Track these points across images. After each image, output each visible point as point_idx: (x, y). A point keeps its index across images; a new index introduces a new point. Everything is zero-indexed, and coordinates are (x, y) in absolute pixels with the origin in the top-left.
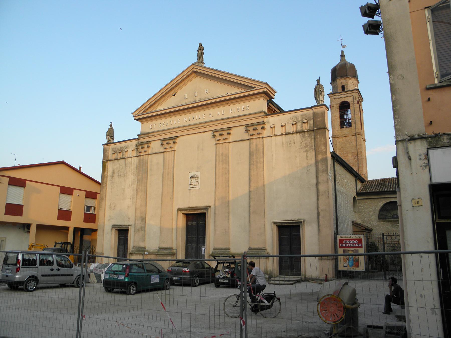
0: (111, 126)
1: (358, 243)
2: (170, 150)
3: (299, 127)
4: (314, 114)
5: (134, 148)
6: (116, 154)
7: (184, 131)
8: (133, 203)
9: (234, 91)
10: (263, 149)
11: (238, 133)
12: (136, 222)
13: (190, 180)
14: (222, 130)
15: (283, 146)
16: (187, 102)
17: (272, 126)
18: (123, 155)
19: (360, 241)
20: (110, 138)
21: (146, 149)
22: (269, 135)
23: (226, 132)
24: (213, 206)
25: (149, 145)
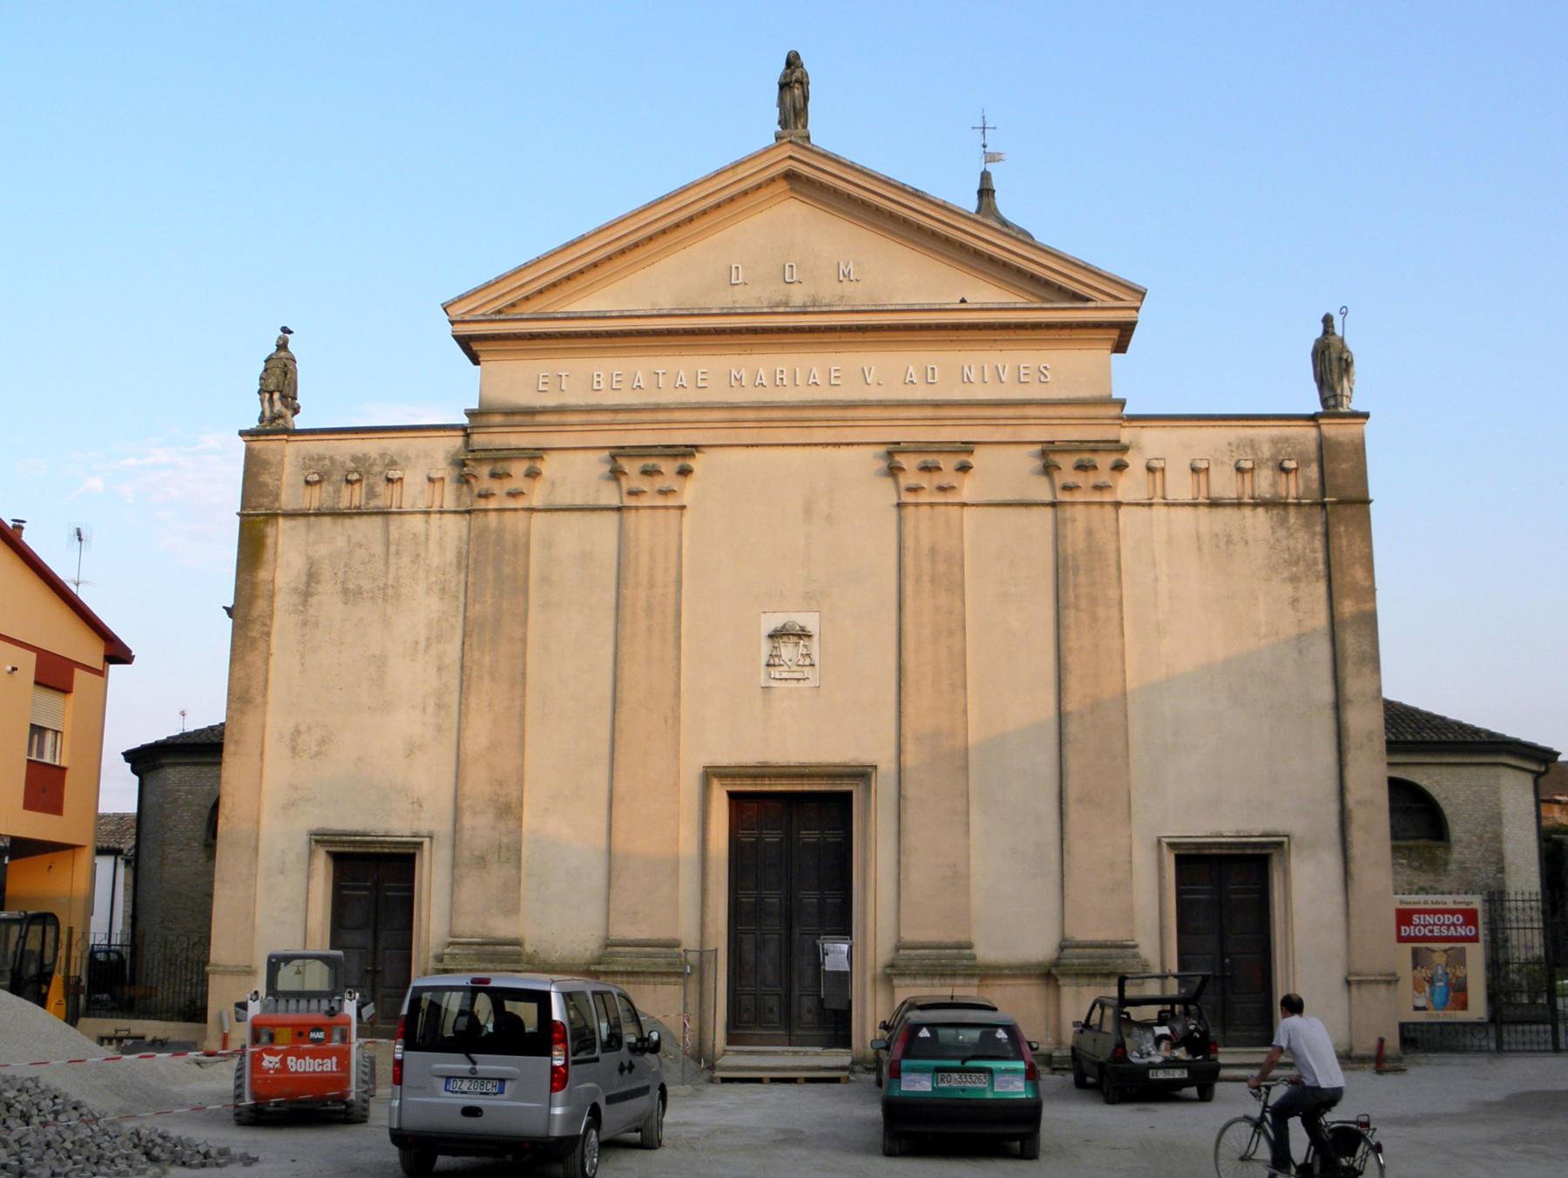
0: (282, 346)
1: (1466, 924)
2: (660, 501)
3: (1264, 483)
4: (1322, 443)
5: (443, 470)
6: (327, 488)
7: (734, 424)
8: (439, 728)
9: (987, 296)
10: (1118, 550)
11: (1005, 469)
12: (467, 821)
13: (765, 647)
14: (935, 448)
15: (1200, 549)
16: (743, 297)
17: (1155, 464)
18: (371, 494)
19: (1470, 917)
20: (278, 406)
21: (517, 481)
22: (1141, 497)
23: (955, 460)
24: (886, 767)
25: (538, 465)
